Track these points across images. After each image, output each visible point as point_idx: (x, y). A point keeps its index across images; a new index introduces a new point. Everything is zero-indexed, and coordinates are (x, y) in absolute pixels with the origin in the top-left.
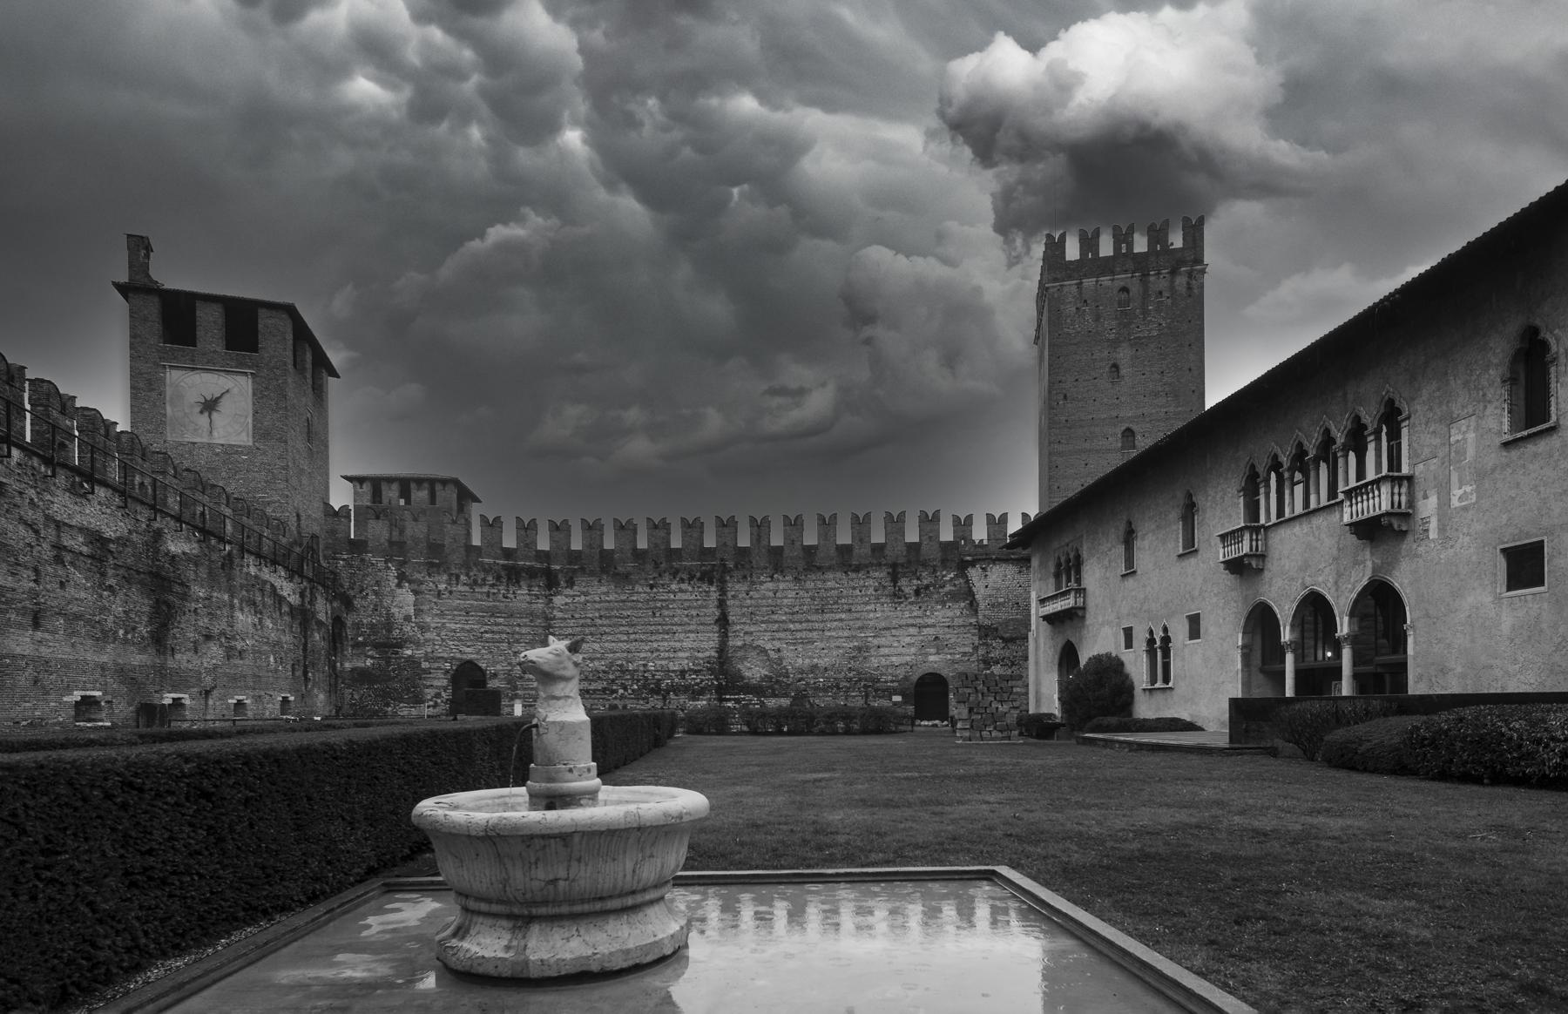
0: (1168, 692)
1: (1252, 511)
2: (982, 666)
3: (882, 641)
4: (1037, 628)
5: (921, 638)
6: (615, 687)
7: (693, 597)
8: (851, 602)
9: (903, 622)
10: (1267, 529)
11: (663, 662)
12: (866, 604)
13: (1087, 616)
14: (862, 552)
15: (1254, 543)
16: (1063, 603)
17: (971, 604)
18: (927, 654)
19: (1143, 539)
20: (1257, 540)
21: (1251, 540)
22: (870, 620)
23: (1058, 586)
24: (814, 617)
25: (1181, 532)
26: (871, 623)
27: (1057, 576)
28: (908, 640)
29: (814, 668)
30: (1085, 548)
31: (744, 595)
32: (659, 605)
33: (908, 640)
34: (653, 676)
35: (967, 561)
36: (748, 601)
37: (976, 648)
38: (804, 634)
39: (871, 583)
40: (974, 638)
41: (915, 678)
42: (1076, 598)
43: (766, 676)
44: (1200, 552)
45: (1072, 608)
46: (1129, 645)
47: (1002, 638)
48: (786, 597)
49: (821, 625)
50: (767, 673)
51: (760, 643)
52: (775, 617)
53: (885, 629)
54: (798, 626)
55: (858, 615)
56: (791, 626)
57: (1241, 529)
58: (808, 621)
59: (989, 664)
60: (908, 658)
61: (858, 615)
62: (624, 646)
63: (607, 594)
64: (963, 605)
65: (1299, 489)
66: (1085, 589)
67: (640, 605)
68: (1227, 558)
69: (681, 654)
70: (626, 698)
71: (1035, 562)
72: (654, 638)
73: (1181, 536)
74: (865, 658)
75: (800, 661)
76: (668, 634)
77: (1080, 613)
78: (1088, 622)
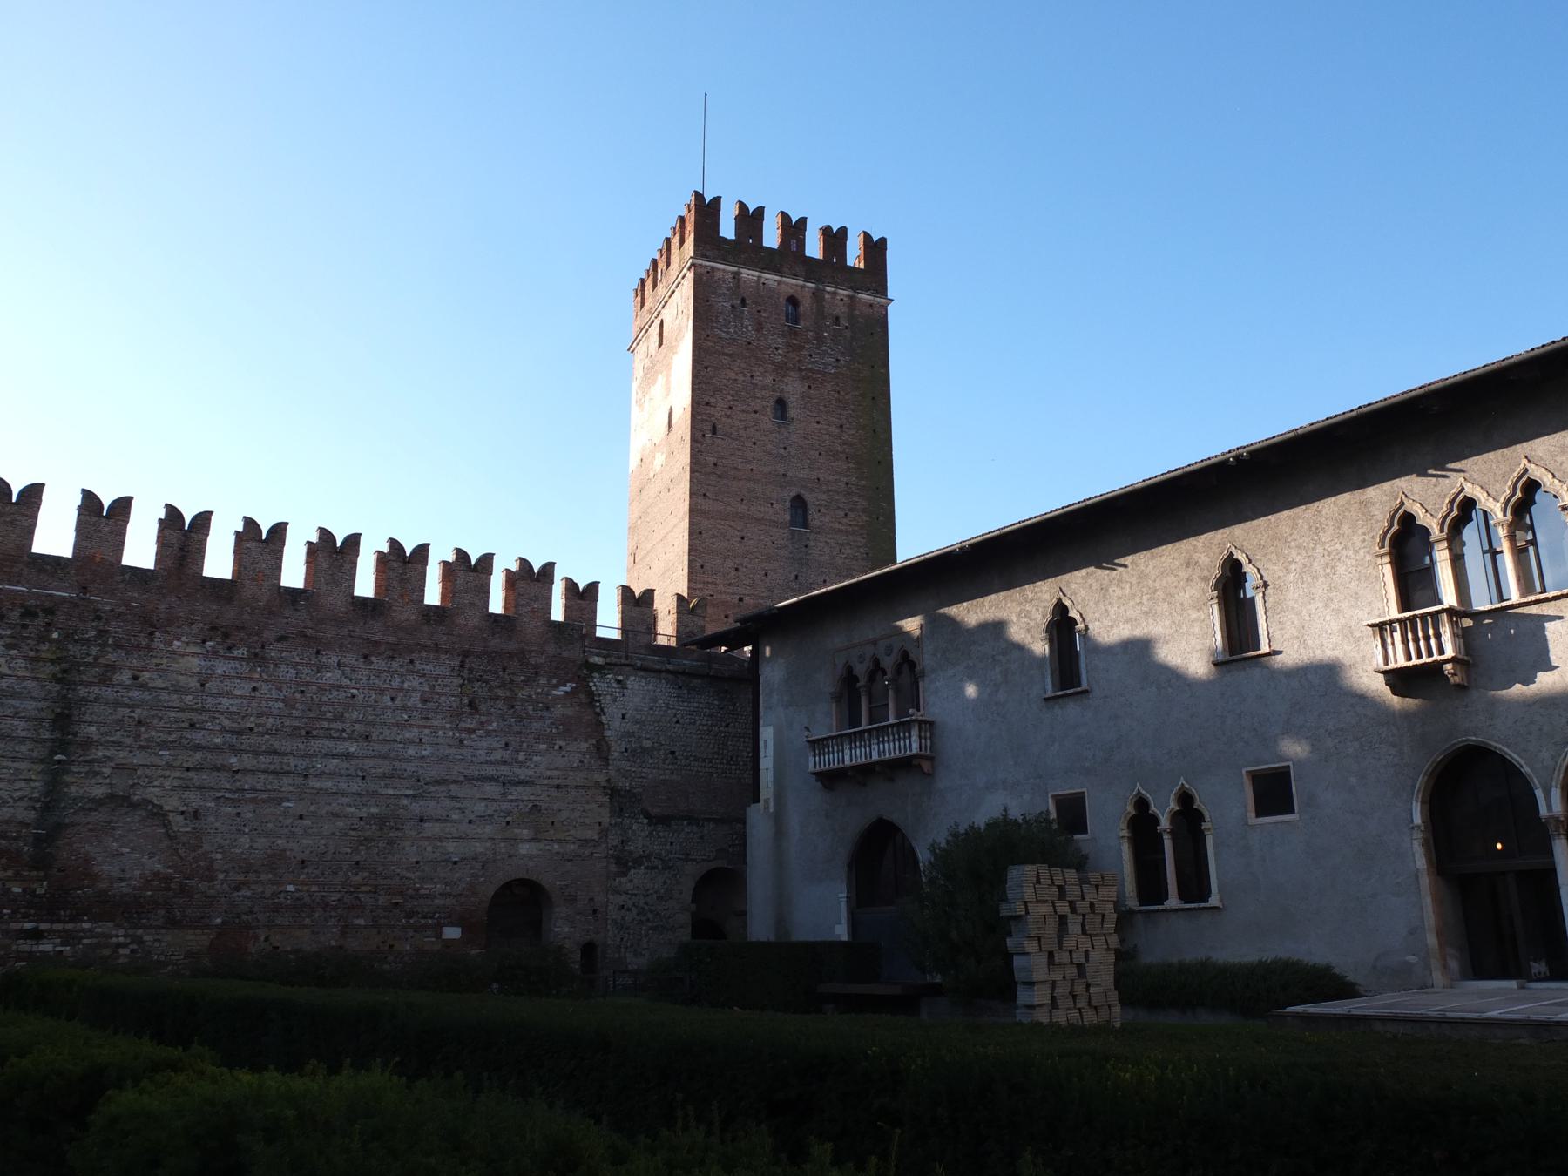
2: (613, 868)
5: (505, 806)
8: (371, 718)
9: (473, 770)
12: (403, 725)
18: (516, 840)
22: (408, 760)
24: (286, 745)
26: (410, 767)
29: (275, 860)
33: (480, 808)
37: (604, 833)
38: (261, 781)
39: (415, 683)
43: (156, 874)
47: (647, 815)
50: (158, 867)
51: (152, 793)
52: (198, 737)
53: (437, 782)
54: (248, 761)
55: (384, 749)
56: (233, 760)
58: (275, 752)
60: (479, 848)
64: (584, 746)
74: (391, 842)
75: (245, 841)
77: (926, 766)
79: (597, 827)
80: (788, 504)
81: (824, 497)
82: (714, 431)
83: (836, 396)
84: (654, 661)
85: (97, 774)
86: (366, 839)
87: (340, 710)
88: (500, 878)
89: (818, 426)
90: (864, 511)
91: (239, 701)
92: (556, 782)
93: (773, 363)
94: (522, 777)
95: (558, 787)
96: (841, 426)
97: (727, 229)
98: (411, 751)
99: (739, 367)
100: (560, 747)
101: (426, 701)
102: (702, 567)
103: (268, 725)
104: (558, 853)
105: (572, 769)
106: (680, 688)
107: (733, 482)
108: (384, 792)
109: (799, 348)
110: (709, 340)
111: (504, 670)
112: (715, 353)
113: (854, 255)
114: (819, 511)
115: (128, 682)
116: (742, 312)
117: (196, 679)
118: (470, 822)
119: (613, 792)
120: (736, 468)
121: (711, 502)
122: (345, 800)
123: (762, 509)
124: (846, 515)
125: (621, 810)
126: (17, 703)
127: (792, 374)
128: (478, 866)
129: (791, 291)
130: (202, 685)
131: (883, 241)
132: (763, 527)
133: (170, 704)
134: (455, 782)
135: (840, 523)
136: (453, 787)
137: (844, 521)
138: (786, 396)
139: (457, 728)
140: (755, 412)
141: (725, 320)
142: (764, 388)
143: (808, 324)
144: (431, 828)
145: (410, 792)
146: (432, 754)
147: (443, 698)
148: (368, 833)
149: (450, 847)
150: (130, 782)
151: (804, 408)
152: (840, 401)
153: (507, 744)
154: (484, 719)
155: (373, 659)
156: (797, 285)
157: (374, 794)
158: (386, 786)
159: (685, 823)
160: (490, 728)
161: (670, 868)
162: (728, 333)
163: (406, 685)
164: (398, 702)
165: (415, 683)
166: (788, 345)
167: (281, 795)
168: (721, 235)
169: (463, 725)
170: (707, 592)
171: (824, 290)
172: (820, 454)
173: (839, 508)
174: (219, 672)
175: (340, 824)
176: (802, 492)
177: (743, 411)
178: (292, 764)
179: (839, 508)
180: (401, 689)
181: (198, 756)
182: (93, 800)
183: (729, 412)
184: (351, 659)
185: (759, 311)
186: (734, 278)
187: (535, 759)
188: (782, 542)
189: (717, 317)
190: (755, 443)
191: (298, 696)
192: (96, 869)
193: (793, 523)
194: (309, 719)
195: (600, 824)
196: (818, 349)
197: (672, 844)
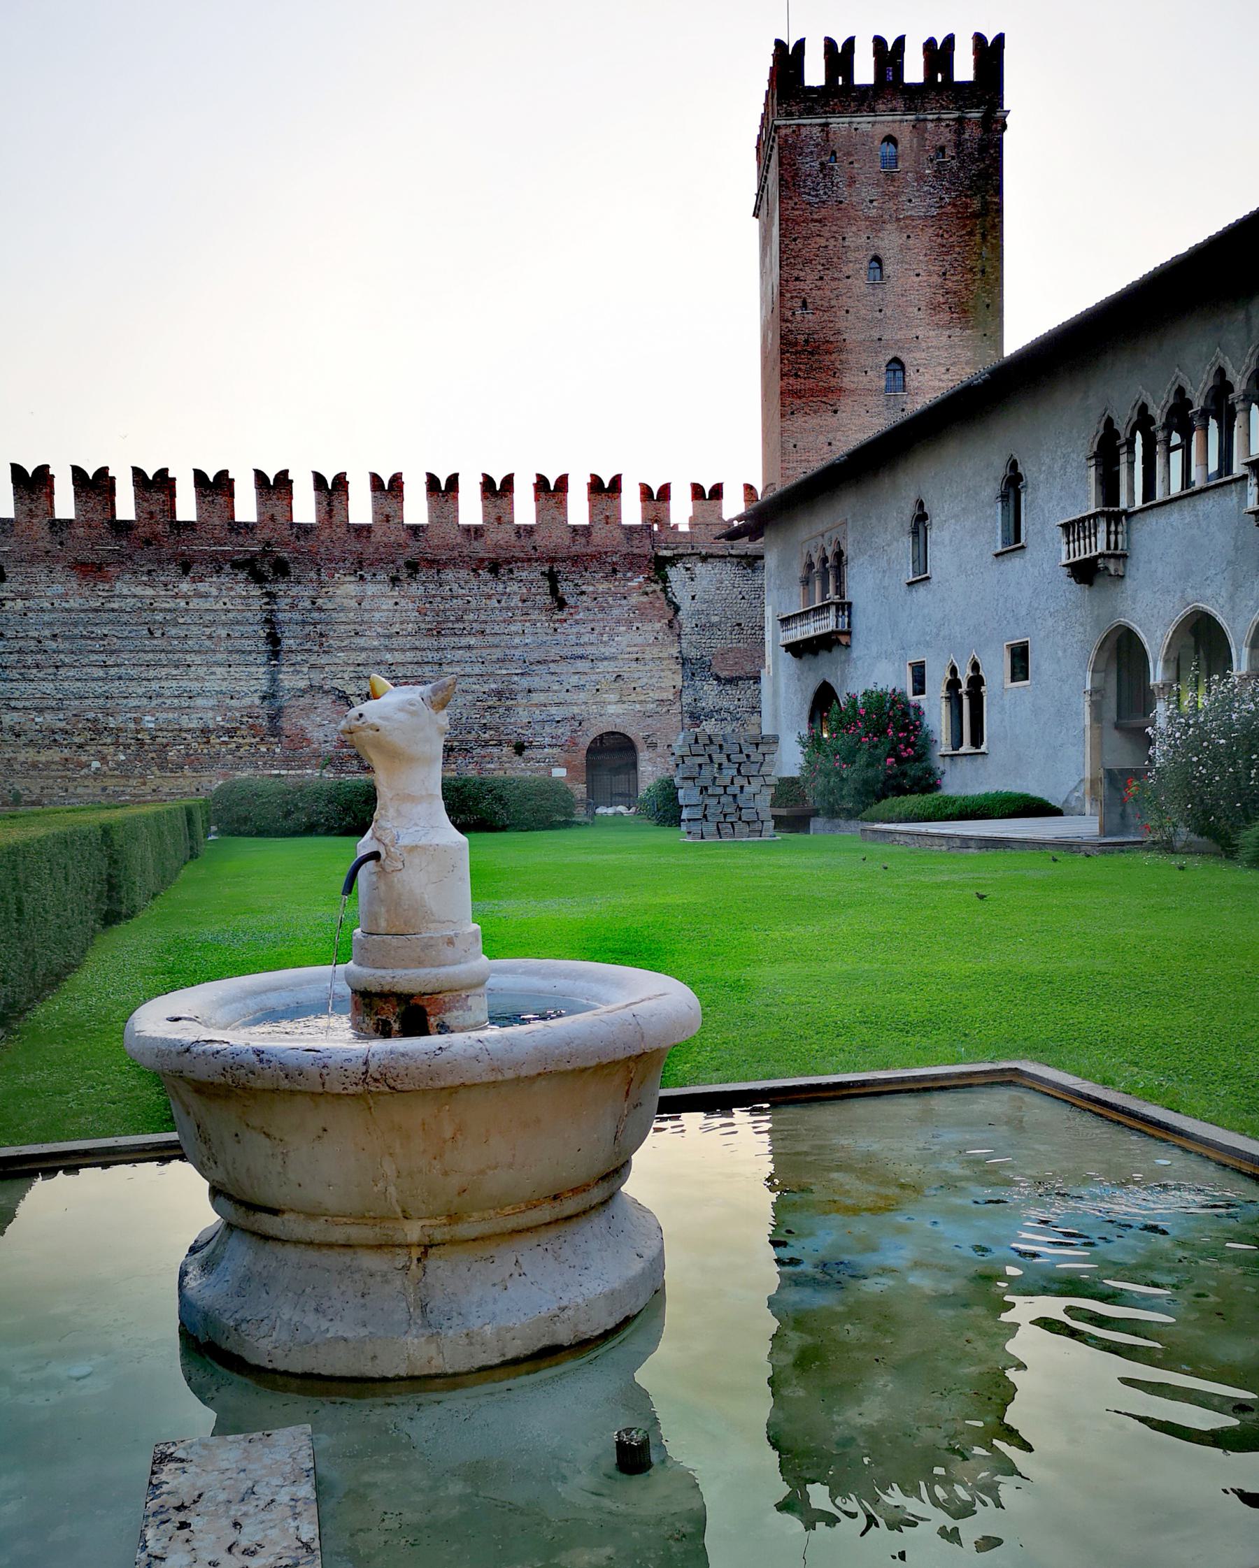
0: (980, 758)
1: (1109, 487)
2: (687, 721)
3: (536, 682)
4: (775, 663)
5: (594, 677)
6: (84, 758)
7: (220, 606)
8: (483, 618)
9: (567, 652)
10: (1129, 515)
11: (171, 716)
12: (508, 622)
13: (854, 644)
14: (498, 536)
15: (1112, 537)
16: (817, 624)
17: (670, 625)
18: (604, 703)
19: (941, 529)
20: (1116, 533)
21: (1109, 533)
23: (808, 598)
25: (999, 517)
26: (517, 653)
27: (806, 582)
28: (575, 680)
30: (850, 539)
31: (307, 604)
32: (159, 617)
33: (575, 680)
34: (154, 738)
35: (665, 558)
36: (315, 615)
39: (515, 588)
40: (675, 676)
41: (585, 741)
42: (837, 617)
44: (1028, 550)
45: (832, 632)
46: (919, 688)
47: (718, 678)
48: (378, 610)
49: (437, 656)
51: (336, 683)
52: (361, 642)
54: (399, 657)
55: (495, 640)
57: (1094, 516)
59: (698, 718)
60: (576, 710)
61: (495, 640)
62: (99, 688)
63: (64, 597)
64: (658, 626)
65: (1176, 457)
66: (850, 604)
67: (126, 617)
68: (1072, 560)
69: (200, 702)
70: (105, 775)
71: (771, 561)
72: (152, 674)
73: (999, 524)
74: (508, 709)
76: (177, 667)
78: (855, 654)
79: (673, 690)
80: (884, 369)
81: (923, 355)
82: (804, 305)
83: (939, 240)
84: (722, 547)
85: (298, 672)
86: (489, 708)
87: (460, 613)
88: (594, 733)
89: (917, 279)
90: (967, 363)
91: (386, 613)
92: (635, 656)
93: (867, 218)
94: (607, 654)
95: (637, 659)
96: (944, 274)
97: (814, 73)
98: (517, 641)
99: (830, 231)
100: (638, 628)
101: (524, 601)
102: (795, 446)
103: (410, 630)
104: (639, 711)
105: (649, 645)
106: (745, 568)
107: (826, 357)
108: (499, 672)
109: (897, 195)
110: (797, 209)
111: (586, 570)
112: (803, 222)
113: (964, 69)
114: (918, 371)
115: (309, 607)
116: (832, 169)
117: (354, 600)
118: (568, 691)
119: (684, 661)
120: (827, 342)
121: (803, 381)
122: (471, 680)
123: (856, 379)
124: (948, 370)
125: (693, 674)
126: (241, 628)
127: (888, 226)
128: (577, 724)
129: (887, 131)
130: (360, 604)
131: (1000, 39)
132: (856, 398)
133: (339, 620)
134: (553, 661)
135: (940, 380)
136: (551, 665)
137: (945, 377)
138: (881, 253)
139: (551, 620)
140: (848, 277)
141: (813, 182)
142: (857, 249)
143: (907, 164)
144: (537, 698)
145: (517, 672)
146: (534, 643)
147: (538, 597)
148: (490, 703)
149: (553, 710)
150: (322, 676)
151: (902, 262)
152: (944, 246)
153: (593, 629)
154: (572, 611)
155: (480, 572)
156: (894, 122)
157: (493, 674)
158: (500, 668)
159: (751, 682)
160: (578, 617)
161: (738, 719)
162: (817, 196)
163: (508, 590)
164: (503, 603)
165: (515, 588)
166: (884, 194)
167: (425, 679)
168: (807, 83)
169: (555, 617)
170: (801, 471)
171: (925, 120)
172: (919, 309)
173: (940, 364)
174: (369, 593)
175: (470, 698)
176: (899, 354)
177: (834, 279)
178: (430, 656)
179: (940, 364)
180: (505, 593)
181: (364, 655)
182: (299, 690)
183: (819, 283)
184: (463, 574)
185: (852, 163)
186: (823, 130)
187: (616, 639)
188: (877, 410)
189: (804, 181)
190: (847, 312)
191: (427, 605)
192: (309, 735)
193: (887, 389)
194: (438, 623)
195: (674, 687)
196: (918, 191)
197: (739, 700)
